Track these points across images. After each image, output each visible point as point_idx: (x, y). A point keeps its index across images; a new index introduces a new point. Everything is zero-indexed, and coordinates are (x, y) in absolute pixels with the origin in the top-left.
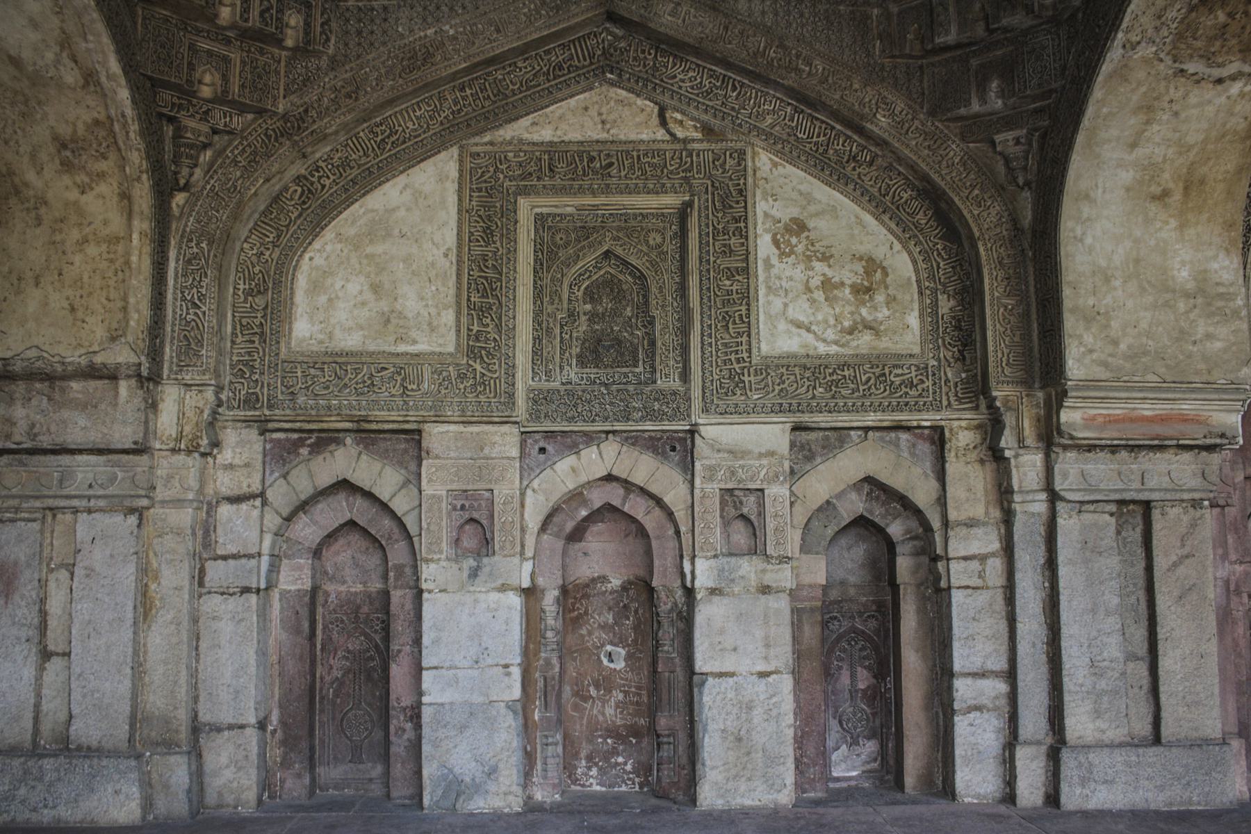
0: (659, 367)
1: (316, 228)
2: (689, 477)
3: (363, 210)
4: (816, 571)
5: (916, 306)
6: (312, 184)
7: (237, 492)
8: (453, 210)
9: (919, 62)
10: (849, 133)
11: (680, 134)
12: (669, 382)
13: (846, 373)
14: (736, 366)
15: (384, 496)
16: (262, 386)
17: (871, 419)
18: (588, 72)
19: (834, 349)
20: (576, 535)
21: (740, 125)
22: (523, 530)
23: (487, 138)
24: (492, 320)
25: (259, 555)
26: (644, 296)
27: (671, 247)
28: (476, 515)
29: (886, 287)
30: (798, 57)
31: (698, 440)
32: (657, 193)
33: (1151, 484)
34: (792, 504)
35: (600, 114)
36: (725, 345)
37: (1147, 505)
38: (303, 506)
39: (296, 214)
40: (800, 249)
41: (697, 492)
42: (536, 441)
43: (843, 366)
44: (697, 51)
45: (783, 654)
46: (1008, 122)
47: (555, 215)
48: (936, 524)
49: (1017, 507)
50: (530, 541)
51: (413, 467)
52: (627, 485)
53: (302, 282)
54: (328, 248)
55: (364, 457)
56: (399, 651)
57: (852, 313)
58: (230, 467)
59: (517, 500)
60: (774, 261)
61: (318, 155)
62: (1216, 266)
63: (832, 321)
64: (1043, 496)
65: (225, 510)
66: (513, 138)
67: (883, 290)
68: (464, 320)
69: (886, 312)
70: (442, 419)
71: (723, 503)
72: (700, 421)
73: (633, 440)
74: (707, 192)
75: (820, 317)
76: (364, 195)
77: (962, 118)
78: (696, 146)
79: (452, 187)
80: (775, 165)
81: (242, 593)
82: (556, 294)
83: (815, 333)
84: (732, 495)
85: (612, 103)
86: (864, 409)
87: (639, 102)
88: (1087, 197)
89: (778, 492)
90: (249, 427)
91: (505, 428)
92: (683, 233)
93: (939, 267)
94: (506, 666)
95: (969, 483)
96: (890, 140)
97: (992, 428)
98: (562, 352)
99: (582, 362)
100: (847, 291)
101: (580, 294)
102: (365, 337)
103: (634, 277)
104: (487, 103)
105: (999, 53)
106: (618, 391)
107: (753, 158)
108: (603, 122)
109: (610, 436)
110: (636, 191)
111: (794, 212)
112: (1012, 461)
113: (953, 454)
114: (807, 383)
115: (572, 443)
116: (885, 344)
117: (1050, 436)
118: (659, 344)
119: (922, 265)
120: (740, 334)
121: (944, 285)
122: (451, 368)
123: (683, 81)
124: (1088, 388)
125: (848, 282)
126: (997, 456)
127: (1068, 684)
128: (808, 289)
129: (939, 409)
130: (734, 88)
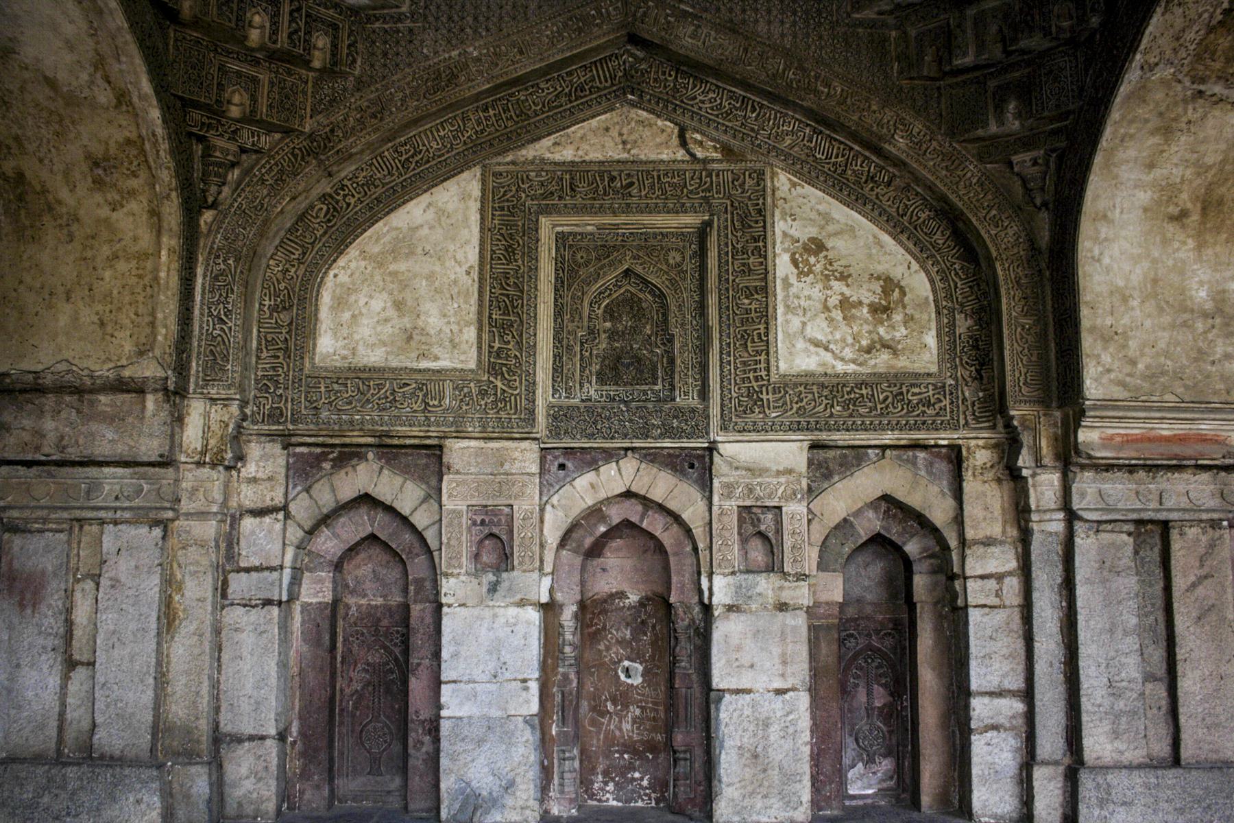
1: (340, 247)
3: (385, 230)
4: (834, 589)
5: (933, 325)
6: (337, 202)
7: (260, 505)
8: (476, 229)
9: (938, 84)
10: (867, 154)
11: (700, 154)
13: (864, 392)
14: (754, 384)
15: (406, 511)
16: (286, 400)
17: (888, 438)
18: (610, 93)
19: (851, 368)
20: (595, 551)
21: (759, 146)
22: (542, 546)
23: (509, 158)
24: (513, 337)
25: (282, 567)
26: (664, 315)
27: (690, 266)
28: (495, 530)
29: (904, 307)
30: (817, 78)
32: (677, 212)
33: (1169, 504)
34: (809, 521)
35: (621, 134)
36: (744, 363)
37: (1165, 526)
38: (325, 520)
39: (321, 232)
40: (818, 268)
41: (715, 508)
42: (556, 458)
43: (860, 385)
44: (717, 73)
45: (800, 671)
46: (1026, 143)
47: (575, 234)
48: (953, 543)
49: (1035, 527)
50: (549, 557)
51: (434, 482)
52: (646, 502)
53: (326, 298)
54: (353, 265)
55: (385, 472)
56: (419, 665)
57: (870, 332)
58: (254, 480)
59: (536, 515)
60: (793, 280)
61: (343, 174)
63: (850, 340)
64: (1061, 515)
65: (248, 523)
67: (900, 309)
68: (485, 337)
69: (904, 331)
70: (462, 435)
71: (741, 521)
72: (719, 439)
73: (651, 457)
74: (726, 212)
75: (838, 336)
76: (388, 213)
77: (979, 139)
78: (715, 166)
79: (474, 206)
80: (794, 185)
81: (264, 605)
82: (577, 312)
83: (833, 352)
84: (750, 513)
85: (633, 124)
86: (882, 428)
87: (659, 123)
88: (1105, 217)
89: (795, 509)
90: (273, 441)
91: (526, 444)
92: (702, 253)
93: (956, 287)
94: (524, 681)
95: (985, 504)
96: (908, 160)
97: (1008, 448)
98: (583, 369)
99: (602, 379)
100: (865, 310)
101: (600, 311)
102: (388, 353)
103: (654, 295)
105: (1016, 74)
107: (772, 179)
108: (624, 143)
109: (629, 453)
110: (655, 210)
111: (813, 232)
112: (1030, 480)
113: (970, 473)
114: (825, 402)
115: (591, 460)
116: (902, 363)
117: (1068, 456)
118: (678, 362)
119: (939, 284)
120: (758, 353)
121: (961, 305)
122: (472, 385)
123: (703, 102)
124: (1105, 408)
125: (866, 301)
126: (1014, 475)
127: (1086, 704)
128: (827, 309)
129: (956, 428)
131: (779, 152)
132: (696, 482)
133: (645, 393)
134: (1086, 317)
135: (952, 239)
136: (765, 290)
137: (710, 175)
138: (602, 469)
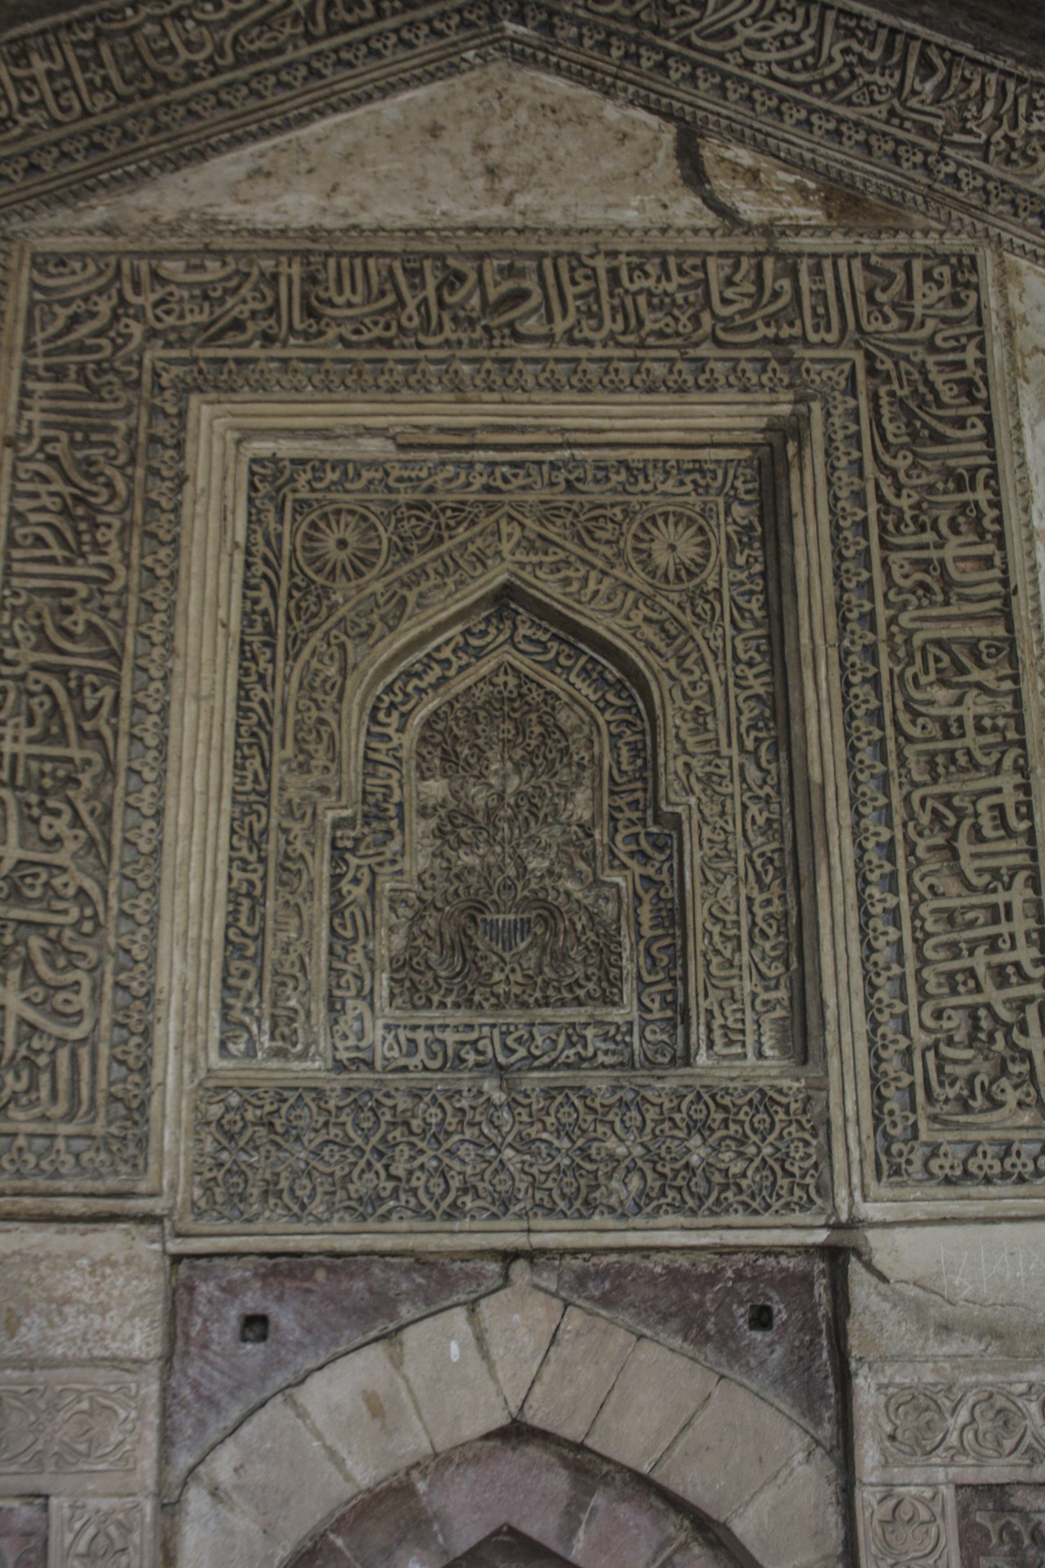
0: (699, 1005)
2: (827, 1431)
11: (751, 208)
14: (992, 994)
21: (954, 179)
23: (92, 218)
24: (77, 821)
26: (636, 750)
27: (731, 575)
35: (481, 147)
36: (949, 917)
41: (866, 1497)
42: (231, 1290)
47: (320, 465)
66: (185, 215)
72: (870, 1211)
73: (604, 1284)
74: (852, 390)
78: (807, 242)
82: (318, 735)
84: (1002, 1508)
85: (522, 116)
87: (611, 111)
91: (109, 1240)
98: (339, 946)
99: (411, 980)
101: (408, 740)
104: (100, 102)
106: (549, 1094)
107: (1002, 288)
108: (491, 172)
109: (519, 1268)
115: (370, 1300)
118: (699, 915)
123: (756, 44)
130: (927, 68)
131: (1017, 201)
132: (782, 1380)
133: (574, 1035)
137: (794, 274)
138: (411, 1336)
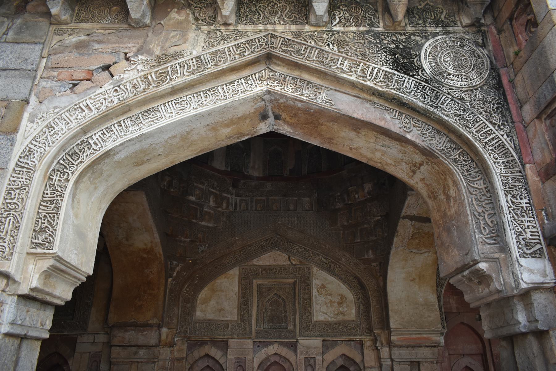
11: (294, 263)
12: (290, 328)
15: (217, 359)
17: (343, 338)
19: (333, 319)
22: (253, 368)
28: (241, 364)
31: (298, 344)
33: (418, 357)
34: (323, 362)
37: (418, 363)
40: (324, 293)
43: (335, 324)
48: (362, 368)
49: (383, 363)
51: (225, 351)
52: (280, 356)
59: (252, 361)
60: (317, 296)
62: (430, 297)
64: (390, 360)
68: (239, 312)
69: (346, 309)
73: (281, 344)
78: (298, 266)
86: (341, 336)
89: (319, 358)
91: (249, 340)
92: (294, 289)
97: (375, 341)
99: (269, 322)
110: (283, 278)
115: (266, 344)
116: (346, 318)
117: (390, 344)
128: (326, 303)
134: (390, 306)
135: (358, 285)
136: (310, 299)
